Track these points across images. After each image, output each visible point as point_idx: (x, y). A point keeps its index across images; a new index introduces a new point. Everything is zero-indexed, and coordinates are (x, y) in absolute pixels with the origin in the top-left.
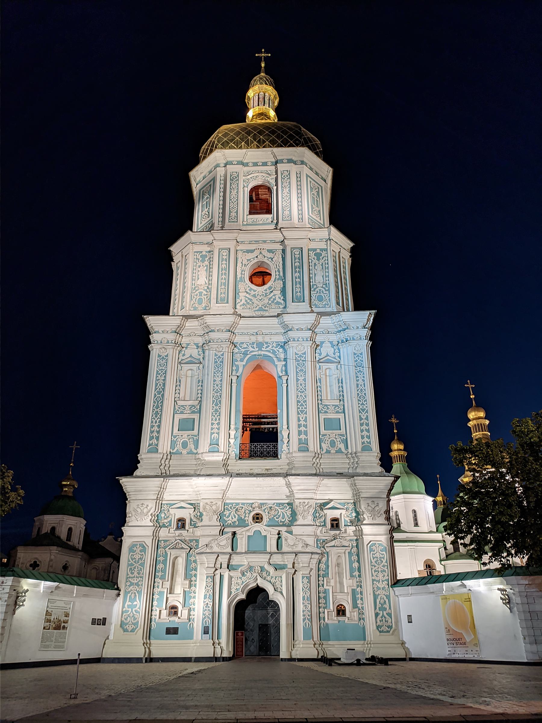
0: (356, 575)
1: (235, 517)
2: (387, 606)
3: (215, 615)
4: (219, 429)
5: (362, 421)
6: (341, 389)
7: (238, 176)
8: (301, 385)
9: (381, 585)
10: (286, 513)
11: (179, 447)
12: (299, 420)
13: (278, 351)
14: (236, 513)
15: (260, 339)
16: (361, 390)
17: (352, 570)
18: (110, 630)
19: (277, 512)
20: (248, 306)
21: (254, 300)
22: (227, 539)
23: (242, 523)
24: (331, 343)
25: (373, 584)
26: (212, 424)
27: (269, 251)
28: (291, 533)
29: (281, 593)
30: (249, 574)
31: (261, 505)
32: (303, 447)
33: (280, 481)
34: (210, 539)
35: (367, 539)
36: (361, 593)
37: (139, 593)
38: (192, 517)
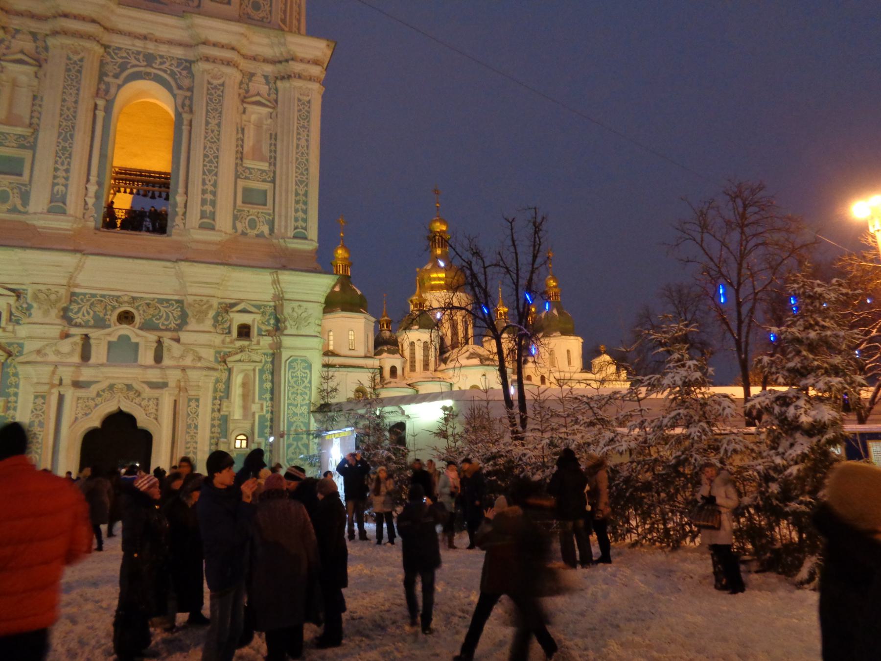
0: (266, 398)
1: (88, 313)
4: (67, 179)
5: (298, 198)
6: (273, 147)
8: (212, 131)
9: (298, 411)
10: (172, 313)
12: (204, 183)
13: (180, 73)
14: (90, 308)
15: (151, 47)
16: (303, 153)
17: (262, 391)
19: (157, 312)
23: (100, 323)
25: (288, 409)
26: (56, 170)
28: (178, 340)
34: (45, 343)
38: (13, 310)
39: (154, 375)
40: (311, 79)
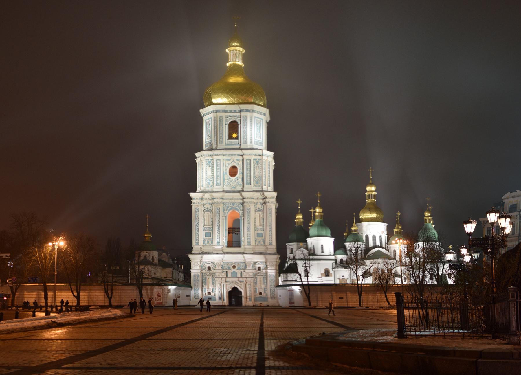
2: (274, 292)
3: (222, 295)
7: (223, 118)
9: (272, 287)
11: (206, 243)
12: (248, 234)
15: (233, 201)
17: (264, 282)
18: (190, 298)
20: (229, 186)
21: (231, 183)
22: (224, 273)
23: (229, 269)
24: (260, 203)
26: (217, 235)
27: (237, 160)
28: (245, 272)
29: (242, 289)
30: (232, 284)
31: (235, 263)
32: (249, 244)
33: (241, 255)
35: (269, 274)
36: (267, 289)
37: (198, 288)
39: (241, 279)
40: (272, 203)
